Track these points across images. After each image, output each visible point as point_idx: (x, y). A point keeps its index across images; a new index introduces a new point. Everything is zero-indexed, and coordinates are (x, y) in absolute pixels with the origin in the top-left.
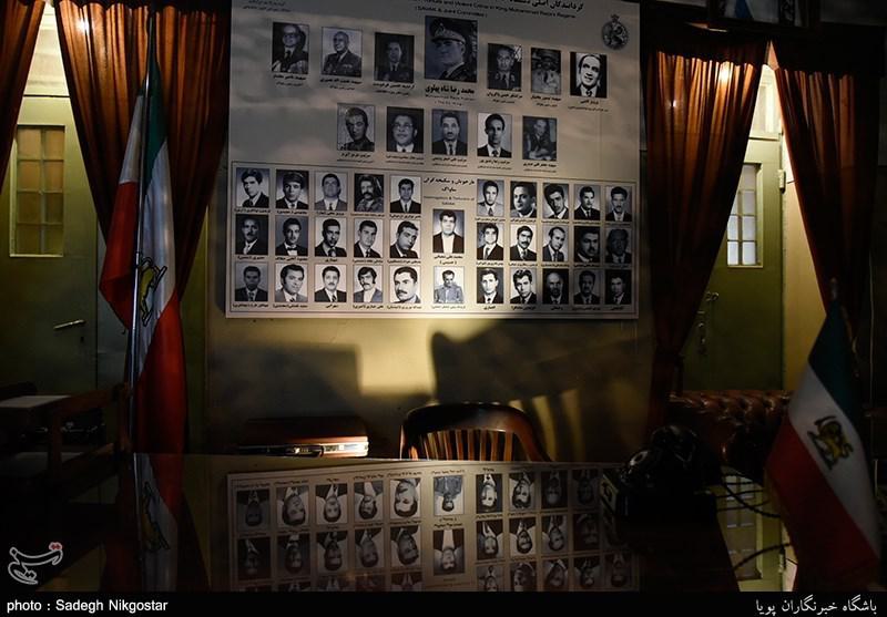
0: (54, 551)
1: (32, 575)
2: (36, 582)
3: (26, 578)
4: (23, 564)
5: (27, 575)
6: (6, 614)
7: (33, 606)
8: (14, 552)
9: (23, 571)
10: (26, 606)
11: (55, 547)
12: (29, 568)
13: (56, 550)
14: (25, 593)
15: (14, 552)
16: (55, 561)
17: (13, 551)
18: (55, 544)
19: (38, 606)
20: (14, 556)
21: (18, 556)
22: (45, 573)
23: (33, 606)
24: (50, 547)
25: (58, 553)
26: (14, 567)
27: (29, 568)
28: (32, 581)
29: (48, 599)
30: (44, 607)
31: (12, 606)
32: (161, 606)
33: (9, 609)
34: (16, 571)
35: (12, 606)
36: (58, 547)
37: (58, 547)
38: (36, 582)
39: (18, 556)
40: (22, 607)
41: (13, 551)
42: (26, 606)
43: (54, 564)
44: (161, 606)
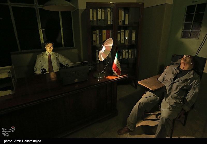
0: (12, 129)
1: (7, 134)
2: (8, 136)
3: (6, 135)
4: (5, 132)
5: (6, 134)
6: (4, 143)
7: (10, 141)
8: (3, 129)
9: (5, 133)
10: (9, 141)
11: (13, 128)
12: (7, 133)
13: (13, 128)
14: (8, 138)
15: (3, 129)
16: (13, 131)
17: (3, 129)
18: (13, 127)
19: (11, 141)
20: (3, 130)
21: (4, 130)
22: (10, 134)
23: (10, 141)
24: (12, 128)
25: (13, 129)
26: (3, 132)
27: (7, 133)
28: (8, 136)
29: (13, 140)
30: (13, 141)
31: (5, 141)
32: (40, 141)
33: (4, 142)
34: (4, 133)
35: (5, 141)
36: (14, 128)
37: (14, 128)
38: (8, 136)
39: (4, 130)
40: (8, 141)
41: (3, 129)
42: (9, 141)
43: (13, 132)
44: (40, 141)
